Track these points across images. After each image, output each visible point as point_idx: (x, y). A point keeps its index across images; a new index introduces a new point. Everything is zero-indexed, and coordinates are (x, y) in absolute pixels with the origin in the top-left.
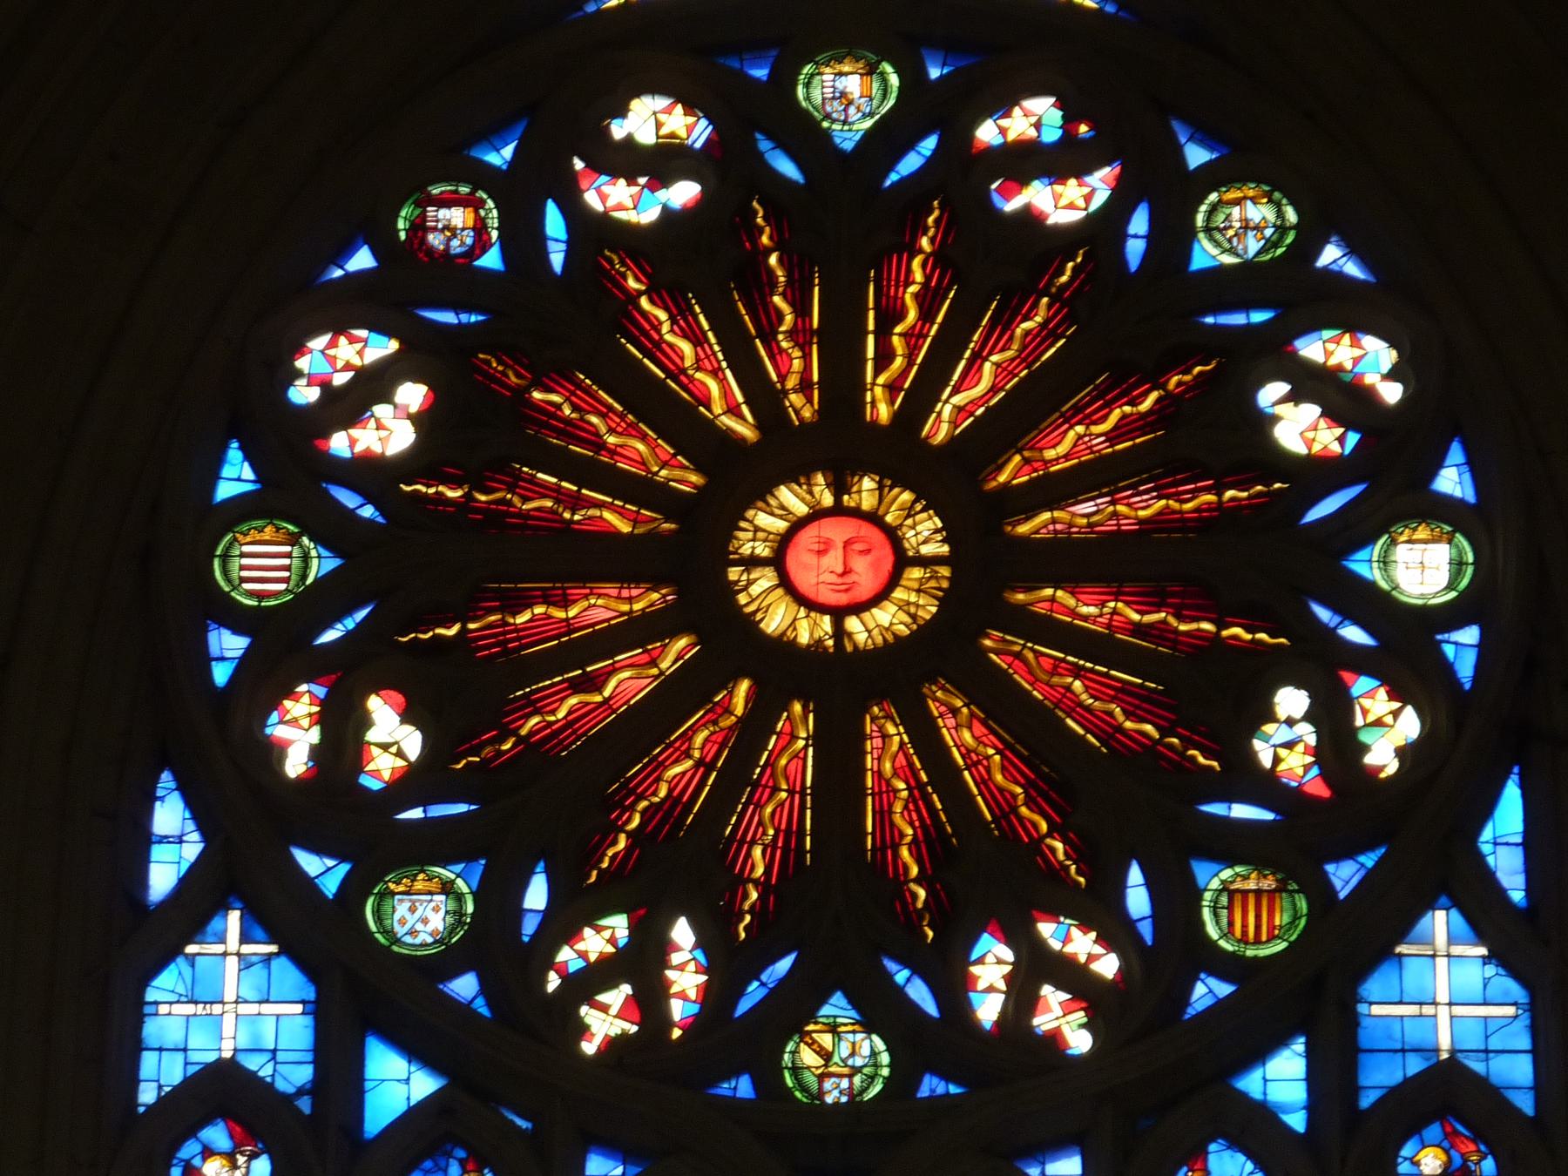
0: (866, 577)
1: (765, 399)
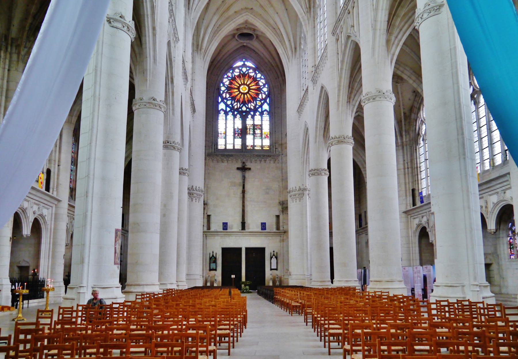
0: (245, 89)
1: (241, 82)
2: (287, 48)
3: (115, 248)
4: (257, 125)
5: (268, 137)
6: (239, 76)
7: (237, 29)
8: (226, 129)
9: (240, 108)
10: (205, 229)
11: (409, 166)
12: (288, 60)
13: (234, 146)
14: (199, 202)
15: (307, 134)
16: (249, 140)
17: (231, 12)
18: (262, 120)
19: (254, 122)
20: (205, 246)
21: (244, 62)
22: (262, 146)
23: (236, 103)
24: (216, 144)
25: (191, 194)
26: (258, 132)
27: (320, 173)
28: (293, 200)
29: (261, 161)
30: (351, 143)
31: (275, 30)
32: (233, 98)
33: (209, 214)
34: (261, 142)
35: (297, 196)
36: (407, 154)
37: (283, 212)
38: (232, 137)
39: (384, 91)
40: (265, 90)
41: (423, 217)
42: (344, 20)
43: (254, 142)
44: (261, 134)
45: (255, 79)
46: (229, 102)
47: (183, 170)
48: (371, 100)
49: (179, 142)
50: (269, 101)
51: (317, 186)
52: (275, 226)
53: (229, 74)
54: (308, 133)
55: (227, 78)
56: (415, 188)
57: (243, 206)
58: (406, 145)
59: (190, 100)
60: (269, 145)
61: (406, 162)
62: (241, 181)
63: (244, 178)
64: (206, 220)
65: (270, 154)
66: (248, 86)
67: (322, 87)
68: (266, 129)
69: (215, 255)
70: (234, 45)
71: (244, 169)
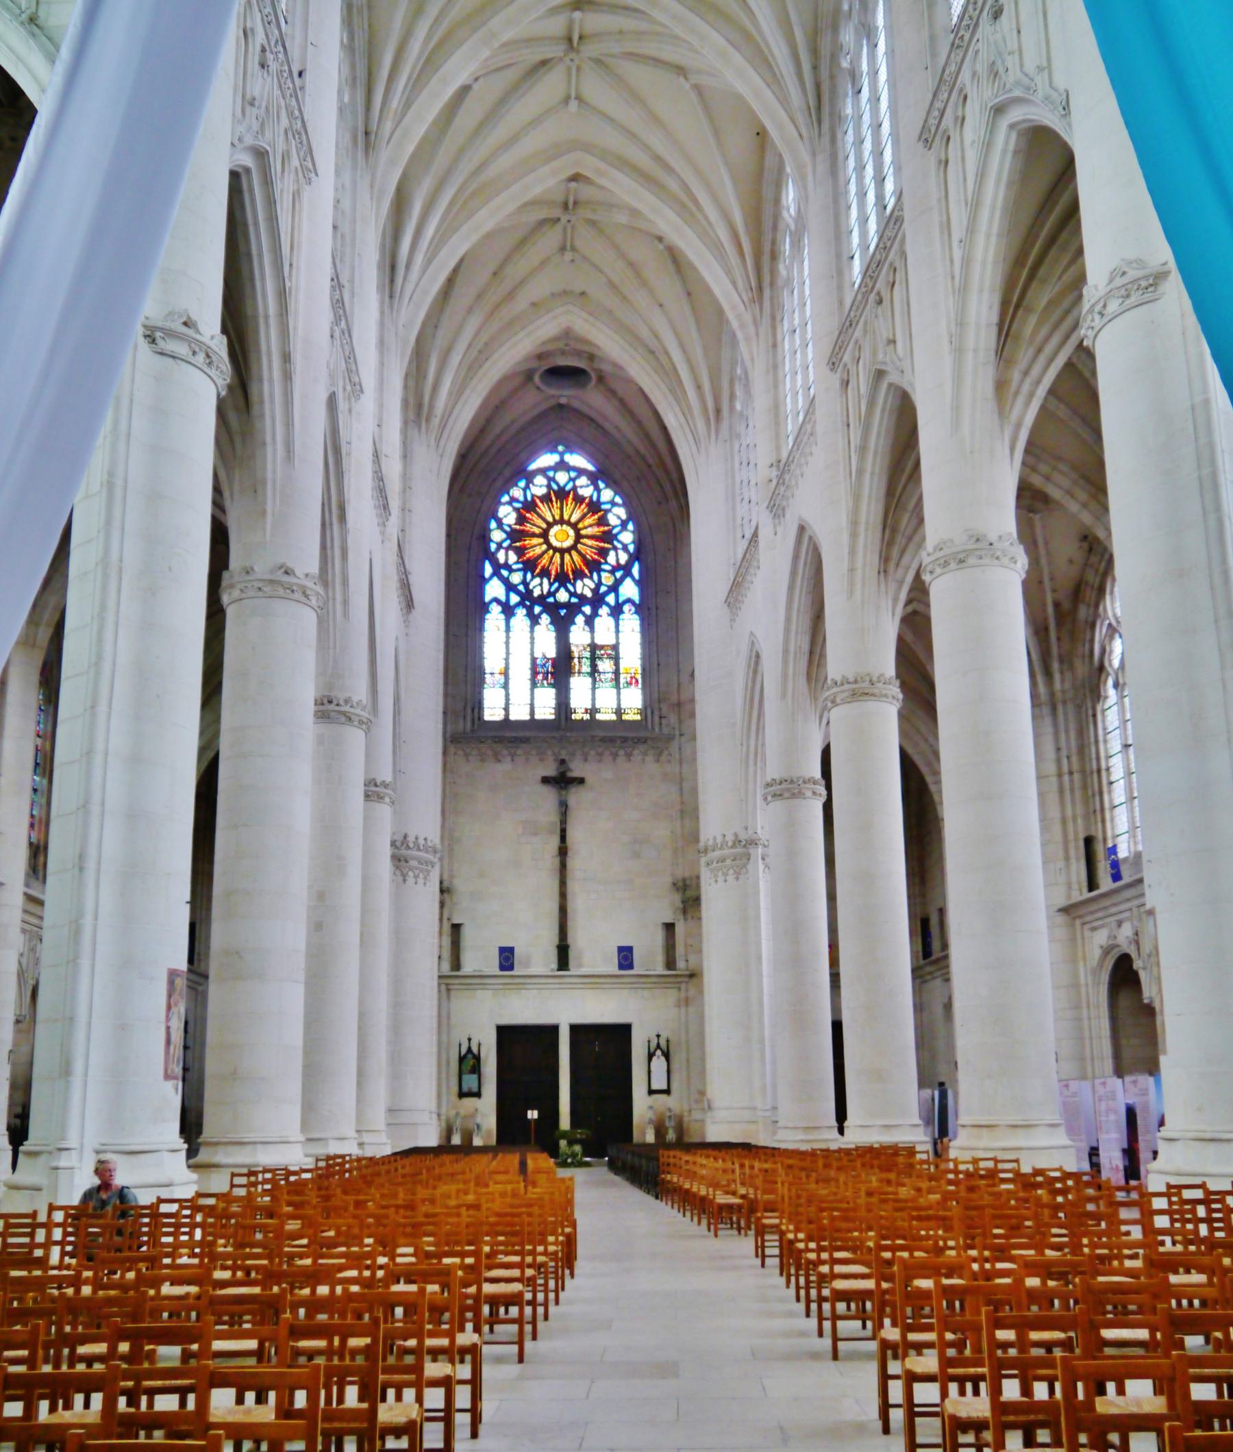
0: (565, 537)
2: (690, 409)
3: (168, 1028)
4: (602, 647)
5: (637, 681)
6: (546, 499)
7: (540, 356)
8: (507, 660)
10: (446, 968)
11: (1075, 766)
12: (694, 447)
13: (532, 712)
14: (425, 884)
15: (755, 672)
16: (580, 693)
17: (521, 303)
19: (593, 638)
20: (444, 1021)
21: (562, 454)
23: (537, 580)
24: (478, 706)
25: (400, 860)
26: (605, 666)
27: (800, 792)
28: (716, 876)
29: (615, 756)
30: (894, 697)
31: (655, 355)
32: (529, 565)
33: (456, 921)
34: (615, 697)
35: (728, 862)
36: (1067, 731)
37: (685, 911)
39: (993, 537)
40: (627, 537)
41: (1120, 924)
42: (866, 323)
43: (594, 699)
44: (617, 673)
45: (594, 506)
46: (516, 578)
47: (376, 785)
48: (953, 565)
49: (364, 702)
51: (791, 829)
52: (660, 958)
54: (760, 668)
55: (510, 503)
56: (1093, 834)
57: (563, 895)
58: (1064, 702)
59: (398, 572)
60: (640, 707)
61: (1064, 753)
62: (555, 818)
64: (447, 941)
65: (643, 734)
66: (574, 526)
67: (802, 529)
68: (632, 657)
69: (475, 1050)
70: (531, 401)
71: (562, 781)
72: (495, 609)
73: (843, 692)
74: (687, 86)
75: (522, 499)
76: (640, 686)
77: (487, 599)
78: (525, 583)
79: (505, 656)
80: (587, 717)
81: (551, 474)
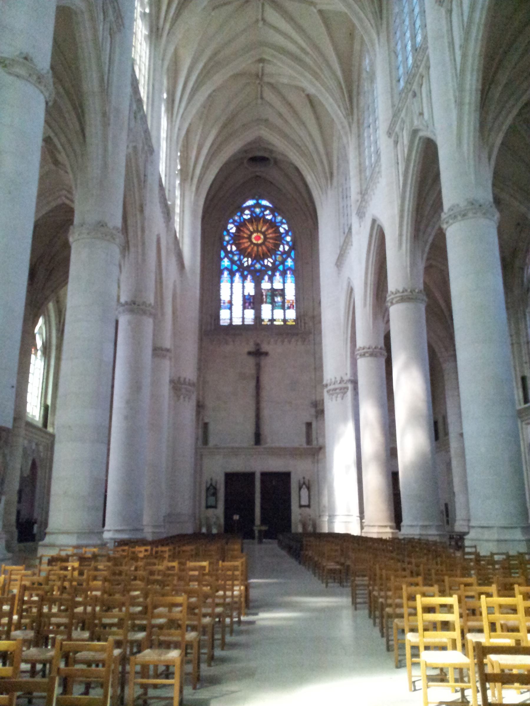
4: (277, 290)
6: (250, 221)
8: (231, 296)
9: (252, 265)
13: (243, 321)
15: (350, 297)
16: (266, 311)
18: (284, 283)
19: (272, 286)
21: (257, 200)
22: (285, 320)
29: (283, 342)
32: (242, 252)
34: (283, 314)
35: (338, 391)
37: (317, 417)
38: (241, 308)
40: (288, 239)
42: (407, 107)
46: (236, 258)
48: (459, 218)
50: (295, 254)
52: (304, 440)
53: (236, 218)
54: (353, 297)
55: (233, 223)
60: (295, 318)
62: (253, 371)
63: (258, 367)
64: (200, 431)
67: (374, 221)
68: (290, 294)
72: (226, 273)
73: (396, 297)
74: (315, 11)
75: (238, 221)
76: (295, 308)
77: (222, 268)
78: (240, 260)
79: (230, 294)
80: (269, 323)
81: (252, 209)
